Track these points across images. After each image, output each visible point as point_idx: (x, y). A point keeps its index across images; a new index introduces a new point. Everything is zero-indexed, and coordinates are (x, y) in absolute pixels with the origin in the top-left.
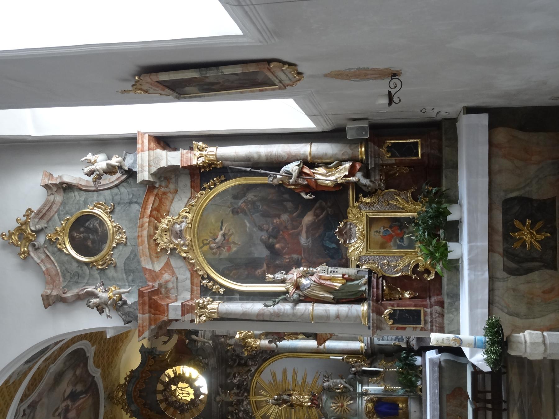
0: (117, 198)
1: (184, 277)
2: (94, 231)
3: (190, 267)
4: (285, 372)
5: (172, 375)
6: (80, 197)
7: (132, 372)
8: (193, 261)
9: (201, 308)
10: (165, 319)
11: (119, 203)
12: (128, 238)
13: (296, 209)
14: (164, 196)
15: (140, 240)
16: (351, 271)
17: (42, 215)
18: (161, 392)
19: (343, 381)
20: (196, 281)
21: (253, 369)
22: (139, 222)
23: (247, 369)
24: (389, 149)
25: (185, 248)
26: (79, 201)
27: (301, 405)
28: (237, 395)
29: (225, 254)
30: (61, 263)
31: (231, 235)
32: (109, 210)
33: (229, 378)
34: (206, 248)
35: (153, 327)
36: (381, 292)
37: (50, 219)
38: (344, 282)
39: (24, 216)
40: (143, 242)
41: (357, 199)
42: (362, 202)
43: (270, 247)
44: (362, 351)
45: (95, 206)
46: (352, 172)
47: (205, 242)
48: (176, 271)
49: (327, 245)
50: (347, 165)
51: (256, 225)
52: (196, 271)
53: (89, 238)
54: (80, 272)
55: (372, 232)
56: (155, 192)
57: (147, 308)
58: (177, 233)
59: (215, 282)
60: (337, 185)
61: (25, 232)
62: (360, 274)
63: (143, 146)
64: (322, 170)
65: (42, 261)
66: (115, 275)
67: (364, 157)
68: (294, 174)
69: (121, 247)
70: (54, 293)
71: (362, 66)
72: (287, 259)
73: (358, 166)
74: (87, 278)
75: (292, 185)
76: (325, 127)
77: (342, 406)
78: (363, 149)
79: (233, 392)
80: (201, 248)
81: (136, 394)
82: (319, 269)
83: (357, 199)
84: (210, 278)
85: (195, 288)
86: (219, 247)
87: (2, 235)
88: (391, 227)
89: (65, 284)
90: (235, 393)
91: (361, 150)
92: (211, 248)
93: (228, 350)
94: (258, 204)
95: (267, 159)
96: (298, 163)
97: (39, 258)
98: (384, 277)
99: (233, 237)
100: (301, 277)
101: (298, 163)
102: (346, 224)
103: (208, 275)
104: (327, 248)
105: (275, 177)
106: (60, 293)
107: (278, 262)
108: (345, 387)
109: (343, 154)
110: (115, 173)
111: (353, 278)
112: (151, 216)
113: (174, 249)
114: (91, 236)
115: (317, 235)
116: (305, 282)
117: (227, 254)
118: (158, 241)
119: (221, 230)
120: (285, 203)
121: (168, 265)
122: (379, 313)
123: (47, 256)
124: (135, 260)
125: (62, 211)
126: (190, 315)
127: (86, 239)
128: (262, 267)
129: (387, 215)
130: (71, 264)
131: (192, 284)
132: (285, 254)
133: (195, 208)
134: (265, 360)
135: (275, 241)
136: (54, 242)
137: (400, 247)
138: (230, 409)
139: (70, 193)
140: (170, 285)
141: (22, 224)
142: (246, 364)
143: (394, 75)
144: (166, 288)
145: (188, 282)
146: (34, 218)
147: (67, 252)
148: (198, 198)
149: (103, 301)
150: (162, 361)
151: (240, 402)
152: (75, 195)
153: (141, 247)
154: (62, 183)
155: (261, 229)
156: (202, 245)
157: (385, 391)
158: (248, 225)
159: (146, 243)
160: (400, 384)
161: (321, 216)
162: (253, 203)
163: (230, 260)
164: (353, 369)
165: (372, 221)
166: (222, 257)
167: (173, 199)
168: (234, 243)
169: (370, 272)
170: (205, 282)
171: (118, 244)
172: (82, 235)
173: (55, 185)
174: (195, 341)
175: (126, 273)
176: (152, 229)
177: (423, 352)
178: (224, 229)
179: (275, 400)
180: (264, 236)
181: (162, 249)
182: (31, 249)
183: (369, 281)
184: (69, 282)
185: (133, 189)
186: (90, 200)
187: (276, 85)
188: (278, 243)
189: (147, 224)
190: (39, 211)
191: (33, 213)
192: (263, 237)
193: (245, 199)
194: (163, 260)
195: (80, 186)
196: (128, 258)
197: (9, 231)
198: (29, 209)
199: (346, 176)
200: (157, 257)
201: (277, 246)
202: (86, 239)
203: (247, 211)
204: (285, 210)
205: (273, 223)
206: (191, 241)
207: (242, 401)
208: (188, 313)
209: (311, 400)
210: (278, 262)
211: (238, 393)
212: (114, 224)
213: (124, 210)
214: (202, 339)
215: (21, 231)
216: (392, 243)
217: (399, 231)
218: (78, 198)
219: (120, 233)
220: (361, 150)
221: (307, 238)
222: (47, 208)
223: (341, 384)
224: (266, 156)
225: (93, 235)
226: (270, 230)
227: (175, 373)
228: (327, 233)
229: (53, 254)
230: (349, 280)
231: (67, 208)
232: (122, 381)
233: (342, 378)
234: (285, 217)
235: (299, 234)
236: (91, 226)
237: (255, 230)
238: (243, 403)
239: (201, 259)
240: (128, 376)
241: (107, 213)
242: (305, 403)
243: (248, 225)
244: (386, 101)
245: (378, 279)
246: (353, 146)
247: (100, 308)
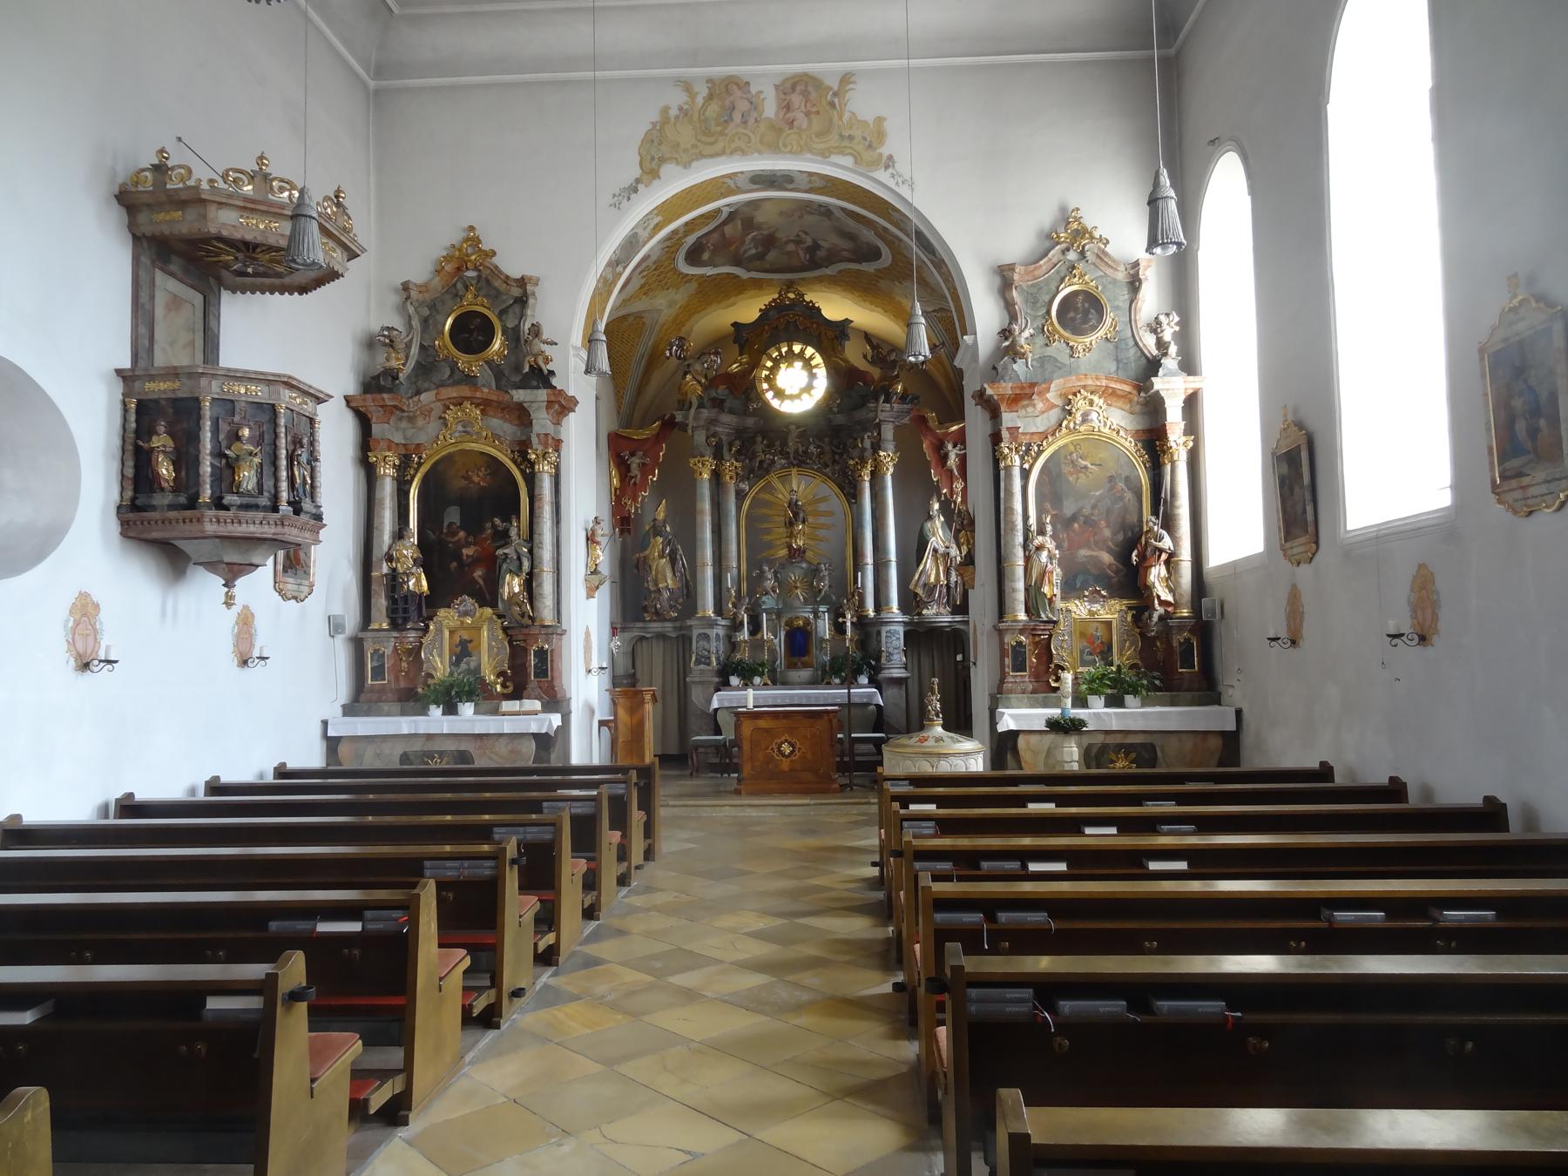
0: (1123, 346)
1: (1038, 424)
2: (1085, 320)
3: (1050, 430)
4: (830, 514)
5: (813, 363)
6: (1123, 302)
7: (819, 310)
8: (1057, 435)
9: (1016, 448)
10: (1002, 409)
11: (1117, 347)
12: (1079, 360)
13: (1117, 545)
14: (1127, 400)
15: (1083, 377)
16: (1059, 604)
17: (1102, 256)
18: (802, 352)
19: (826, 588)
20: (1036, 439)
21: (828, 470)
22: (1102, 375)
23: (830, 463)
24: (1187, 640)
25: (1072, 425)
26: (1118, 300)
27: (791, 535)
28: (796, 452)
29: (1066, 469)
30: (1047, 281)
31: (1086, 474)
32: (1109, 336)
33: (815, 440)
34: (1072, 448)
35: (996, 397)
36: (1040, 633)
37: (1097, 267)
38: (1049, 597)
39: (1101, 236)
40: (1080, 380)
41: (1130, 608)
42: (1126, 613)
43: (1074, 518)
44: (863, 611)
45: (1113, 320)
46: (1163, 603)
47: (1078, 447)
48: (1045, 415)
49: (1079, 577)
50: (1170, 598)
51: (1098, 501)
52: (1047, 438)
53: (1077, 314)
54: (1039, 305)
55: (1096, 624)
56: (1135, 392)
57: (1018, 392)
58: (1088, 415)
59: (1035, 459)
60: (1149, 588)
61: (1082, 238)
62: (1056, 612)
63: (1189, 382)
64: (1164, 572)
65: (1050, 259)
66: (1038, 346)
67: (1178, 615)
68: (1160, 544)
69: (1068, 351)
70: (1016, 277)
71: (1305, 615)
72: (1062, 535)
73: (1170, 609)
74: (1032, 313)
75: (1147, 542)
76: (1208, 577)
77: (796, 588)
78: (1186, 615)
79: (800, 446)
80: (1072, 442)
81: (791, 316)
82: (1059, 570)
83: (1130, 608)
84: (1040, 453)
85: (1028, 437)
86: (1072, 462)
87: (1078, 209)
88: (1102, 643)
89: (1025, 288)
90: (798, 449)
91: (1185, 612)
92: (1071, 453)
93: (856, 439)
94: (1120, 505)
95: (1174, 515)
96: (1172, 548)
97: (1053, 256)
98: (1051, 636)
99: (1084, 477)
100: (1049, 551)
101: (1172, 548)
102: (1104, 597)
103: (1043, 451)
104: (1075, 577)
105: (1155, 524)
106: (1016, 284)
107: (1059, 526)
108: (820, 591)
109: (1182, 594)
110: (1158, 349)
111: (1052, 605)
112: (1107, 387)
113: (1070, 413)
114: (1079, 316)
115: (1089, 567)
116: (1044, 555)
117: (1066, 471)
118: (1078, 395)
119: (1092, 465)
120: (1122, 533)
121: (1054, 406)
122: (1022, 632)
123: (1055, 265)
124: (1056, 369)
125: (1107, 280)
126: (1008, 436)
127: (1076, 310)
128: (1054, 509)
129: (1115, 638)
130: (1047, 294)
131: (1033, 434)
132: (1068, 534)
133: (1115, 435)
134: (842, 488)
135: (1081, 523)
136: (1071, 272)
137: (1082, 652)
138: (778, 443)
139: (1126, 289)
140: (1030, 409)
141: (1091, 233)
142: (834, 462)
143: (1294, 642)
144: (1028, 406)
145: (1034, 430)
146: (1099, 248)
147: (1060, 288)
148: (1126, 439)
149: (1017, 338)
150: (833, 349)
151: (785, 455)
152: (1124, 295)
153: (1074, 378)
154: (1140, 281)
155: (1094, 507)
156: (1075, 443)
157: (822, 640)
158: (1097, 493)
159: (1079, 384)
160: (833, 659)
161: (1109, 572)
162: (1121, 498)
163: (1060, 474)
164: (845, 601)
165: (1108, 624)
166: (1063, 466)
167: (1122, 409)
168: (1078, 478)
169: (1055, 622)
170: (1036, 449)
171: (1072, 348)
172: (1079, 305)
173: (1138, 273)
174: (877, 400)
175: (1040, 358)
176: (1093, 388)
177: (874, 685)
178: (1093, 467)
179: (797, 501)
180: (1086, 511)
181: (1070, 400)
182: (1064, 245)
183: (1050, 622)
184: (1028, 292)
185: (1133, 364)
186: (1119, 312)
187: (1285, 542)
188: (1080, 526)
189: (1099, 384)
190: (1106, 254)
191: (1103, 247)
192: (1085, 510)
193: (1126, 490)
194: (1059, 402)
195: (1136, 302)
196: (1055, 359)
197: (1081, 217)
198: (1108, 242)
199: (1159, 597)
200: (1061, 395)
201: (1076, 525)
202: (1076, 310)
203: (1112, 492)
204: (1115, 534)
205: (1100, 520)
206: (1080, 432)
207: (787, 458)
208: (1010, 434)
209: (799, 549)
210: (1059, 526)
211: (798, 453)
212: (1093, 342)
213: (1109, 354)
214: (880, 409)
215: (1082, 233)
216: (1085, 644)
217: (1098, 651)
218: (1122, 298)
219: (1084, 350)
220: (1185, 612)
221: (1086, 557)
222: (1110, 263)
223: (824, 585)
224: (1178, 515)
225: (1080, 318)
226: (1093, 518)
227: (816, 366)
228: (1090, 577)
229: (1058, 272)
230: (1051, 601)
231: (1110, 286)
232: (807, 298)
233: (830, 586)
234: (1107, 533)
235: (1089, 548)
236: (1090, 316)
237: (1093, 501)
238: (783, 459)
239: (1060, 443)
240: (814, 304)
241: (1106, 334)
242: (796, 541)
243: (1097, 493)
244: (1272, 635)
245: (1049, 630)
246: (1189, 604)
247: (1006, 333)
